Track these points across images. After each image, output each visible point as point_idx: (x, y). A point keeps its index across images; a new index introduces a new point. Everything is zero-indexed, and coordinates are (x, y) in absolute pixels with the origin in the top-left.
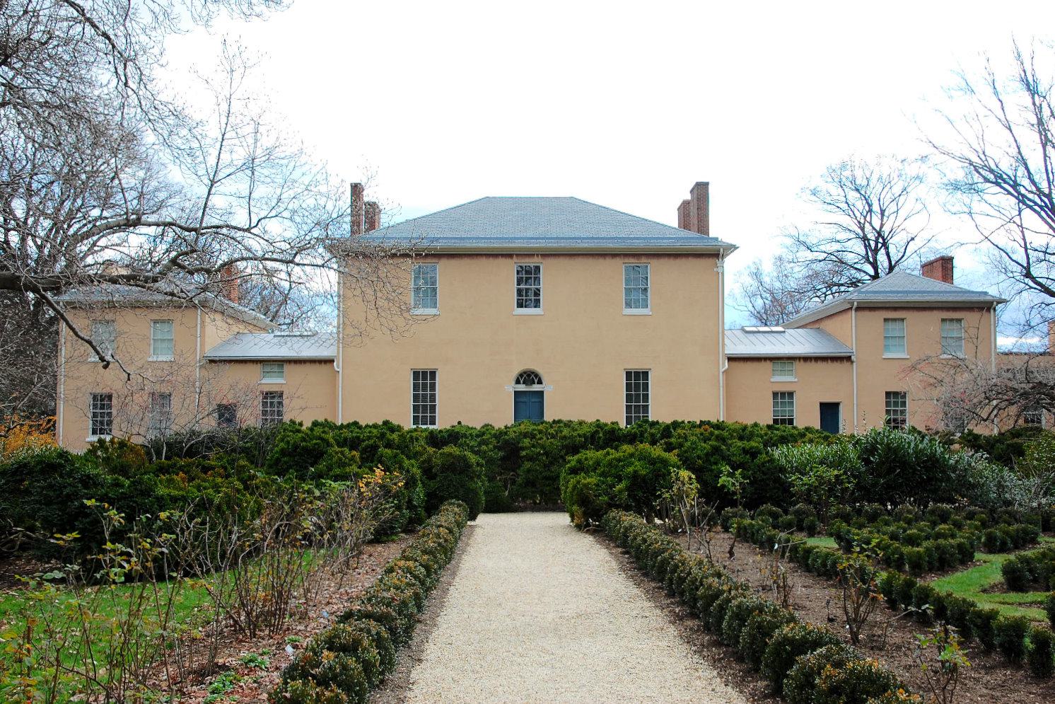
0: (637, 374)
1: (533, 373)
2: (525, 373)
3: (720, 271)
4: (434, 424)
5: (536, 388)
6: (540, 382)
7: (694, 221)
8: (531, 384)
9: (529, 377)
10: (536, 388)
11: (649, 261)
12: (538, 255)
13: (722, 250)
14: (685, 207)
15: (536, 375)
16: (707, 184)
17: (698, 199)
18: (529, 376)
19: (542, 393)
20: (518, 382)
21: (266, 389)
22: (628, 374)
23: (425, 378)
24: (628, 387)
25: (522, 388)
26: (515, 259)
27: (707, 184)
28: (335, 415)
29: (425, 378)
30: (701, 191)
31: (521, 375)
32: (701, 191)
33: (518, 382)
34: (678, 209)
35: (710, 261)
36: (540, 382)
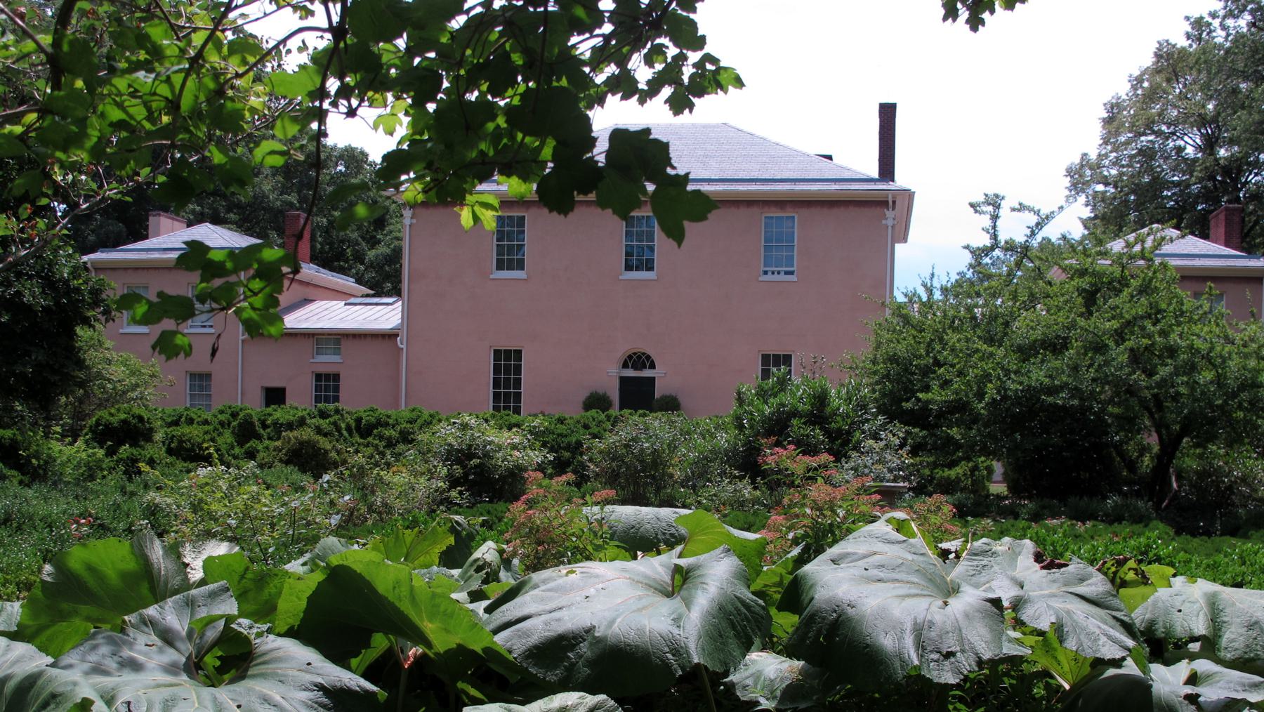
1: (644, 354)
2: (635, 354)
3: (890, 222)
4: (519, 414)
5: (647, 373)
6: (653, 366)
9: (639, 360)
10: (647, 373)
13: (890, 197)
15: (648, 357)
18: (639, 357)
19: (652, 380)
20: (625, 365)
21: (322, 370)
23: (508, 358)
25: (630, 373)
28: (396, 405)
29: (508, 358)
31: (630, 357)
32: (888, 113)
33: (625, 365)
35: (876, 211)
36: (653, 366)
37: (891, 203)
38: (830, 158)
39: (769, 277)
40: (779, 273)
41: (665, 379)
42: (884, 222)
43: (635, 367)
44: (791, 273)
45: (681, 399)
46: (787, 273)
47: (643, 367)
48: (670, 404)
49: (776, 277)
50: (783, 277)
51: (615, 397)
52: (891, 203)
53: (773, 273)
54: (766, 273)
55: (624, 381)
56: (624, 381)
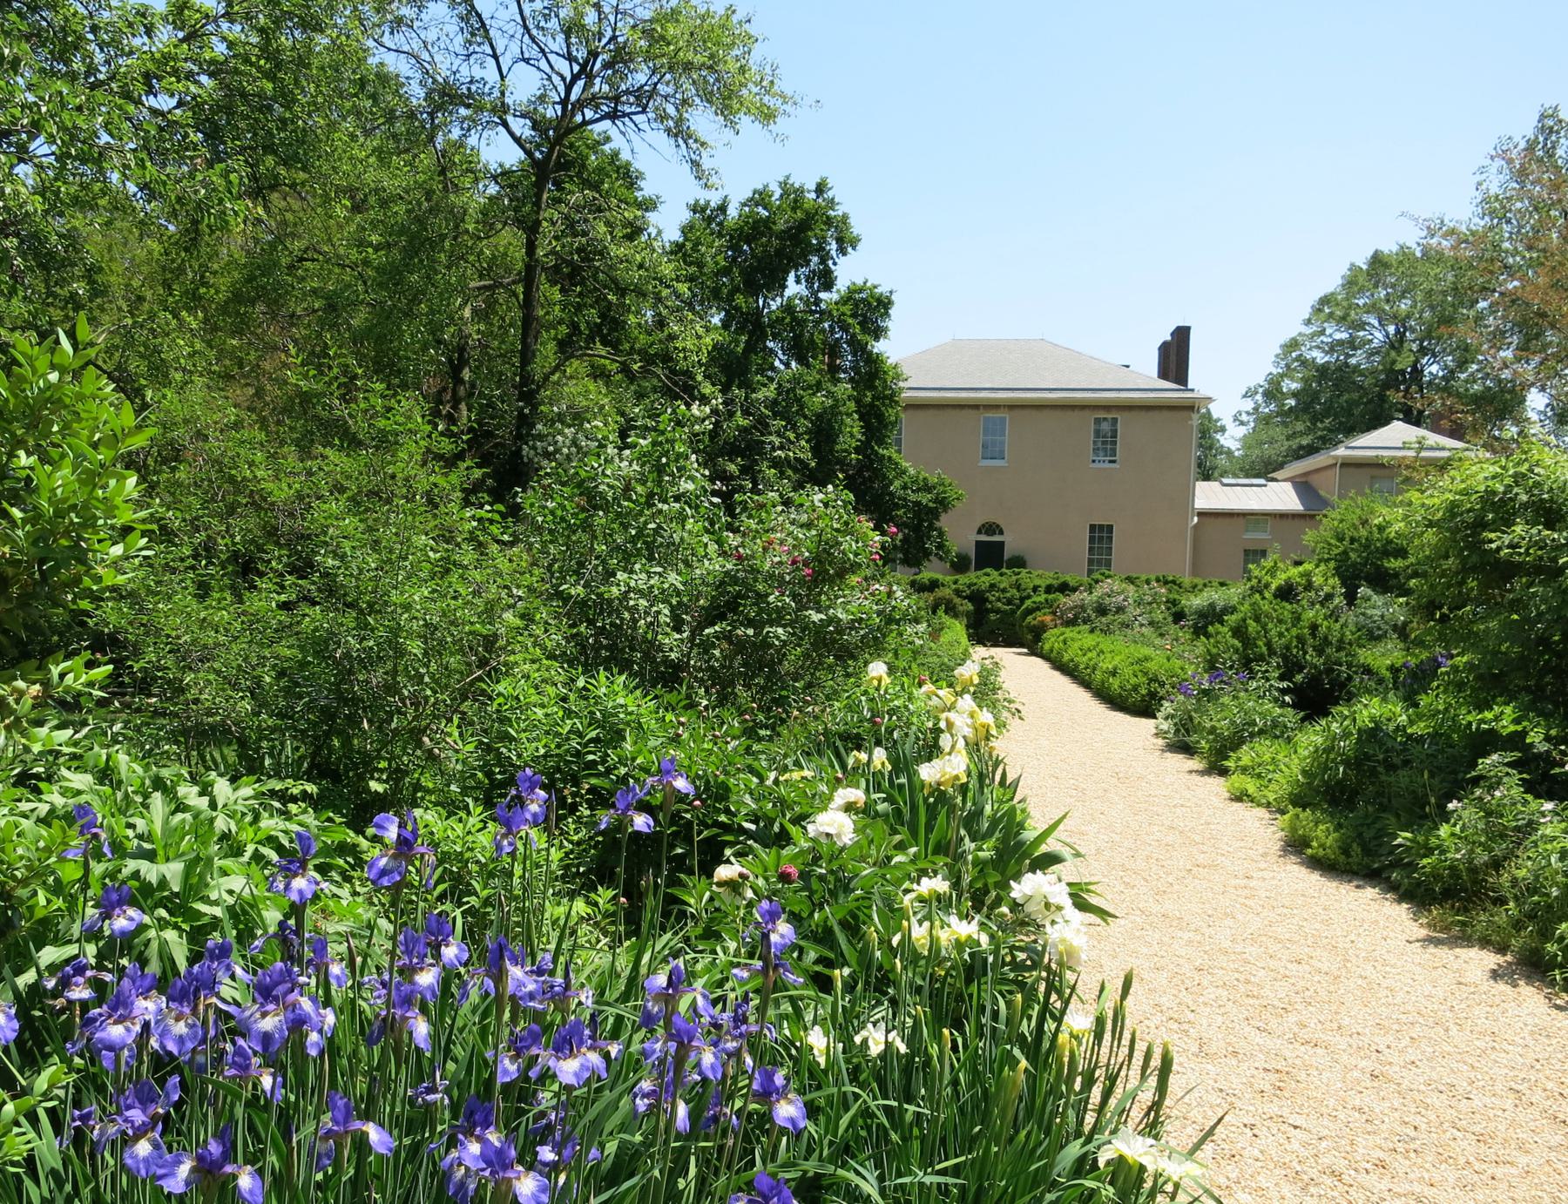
0: (1101, 527)
6: (1001, 533)
7: (1173, 366)
9: (990, 528)
10: (996, 538)
14: (1165, 349)
16: (1187, 329)
20: (979, 532)
22: (1092, 527)
24: (1092, 540)
27: (1187, 329)
30: (1182, 336)
32: (1182, 336)
33: (979, 532)
35: (1185, 414)
36: (1001, 533)
41: (1012, 542)
43: (987, 533)
45: (1027, 558)
47: (993, 533)
48: (1019, 562)
49: (1102, 465)
50: (1107, 465)
55: (978, 543)
56: (978, 543)
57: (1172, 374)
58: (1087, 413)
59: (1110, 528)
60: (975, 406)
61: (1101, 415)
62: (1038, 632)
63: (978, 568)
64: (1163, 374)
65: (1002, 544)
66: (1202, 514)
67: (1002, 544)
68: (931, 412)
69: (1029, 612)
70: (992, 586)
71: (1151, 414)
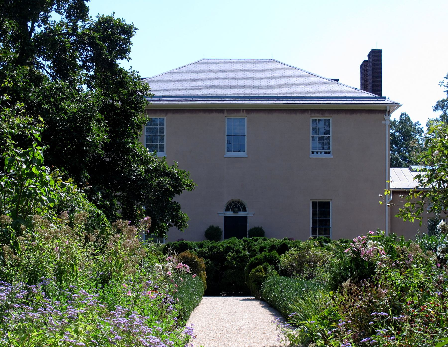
0: (321, 203)
1: (239, 202)
2: (233, 202)
6: (245, 209)
7: (370, 80)
8: (237, 212)
10: (241, 214)
11: (331, 115)
12: (243, 110)
14: (364, 66)
15: (242, 204)
16: (380, 52)
17: (373, 64)
18: (236, 205)
20: (227, 209)
24: (314, 214)
25: (230, 214)
26: (226, 114)
27: (380, 52)
31: (230, 204)
33: (227, 209)
34: (361, 67)
35: (380, 116)
36: (245, 209)
37: (388, 111)
38: (337, 80)
39: (315, 155)
40: (321, 153)
42: (383, 122)
44: (329, 153)
45: (264, 229)
46: (326, 153)
49: (319, 155)
51: (222, 228)
52: (388, 111)
53: (317, 153)
54: (313, 153)
55: (226, 218)
56: (226, 218)
57: (370, 87)
58: (306, 115)
59: (327, 204)
60: (220, 110)
61: (317, 116)
62: (259, 282)
63: (227, 237)
64: (364, 87)
65: (245, 218)
66: (396, 192)
67: (245, 219)
68: (187, 116)
69: (253, 265)
70: (228, 249)
71: (354, 116)
